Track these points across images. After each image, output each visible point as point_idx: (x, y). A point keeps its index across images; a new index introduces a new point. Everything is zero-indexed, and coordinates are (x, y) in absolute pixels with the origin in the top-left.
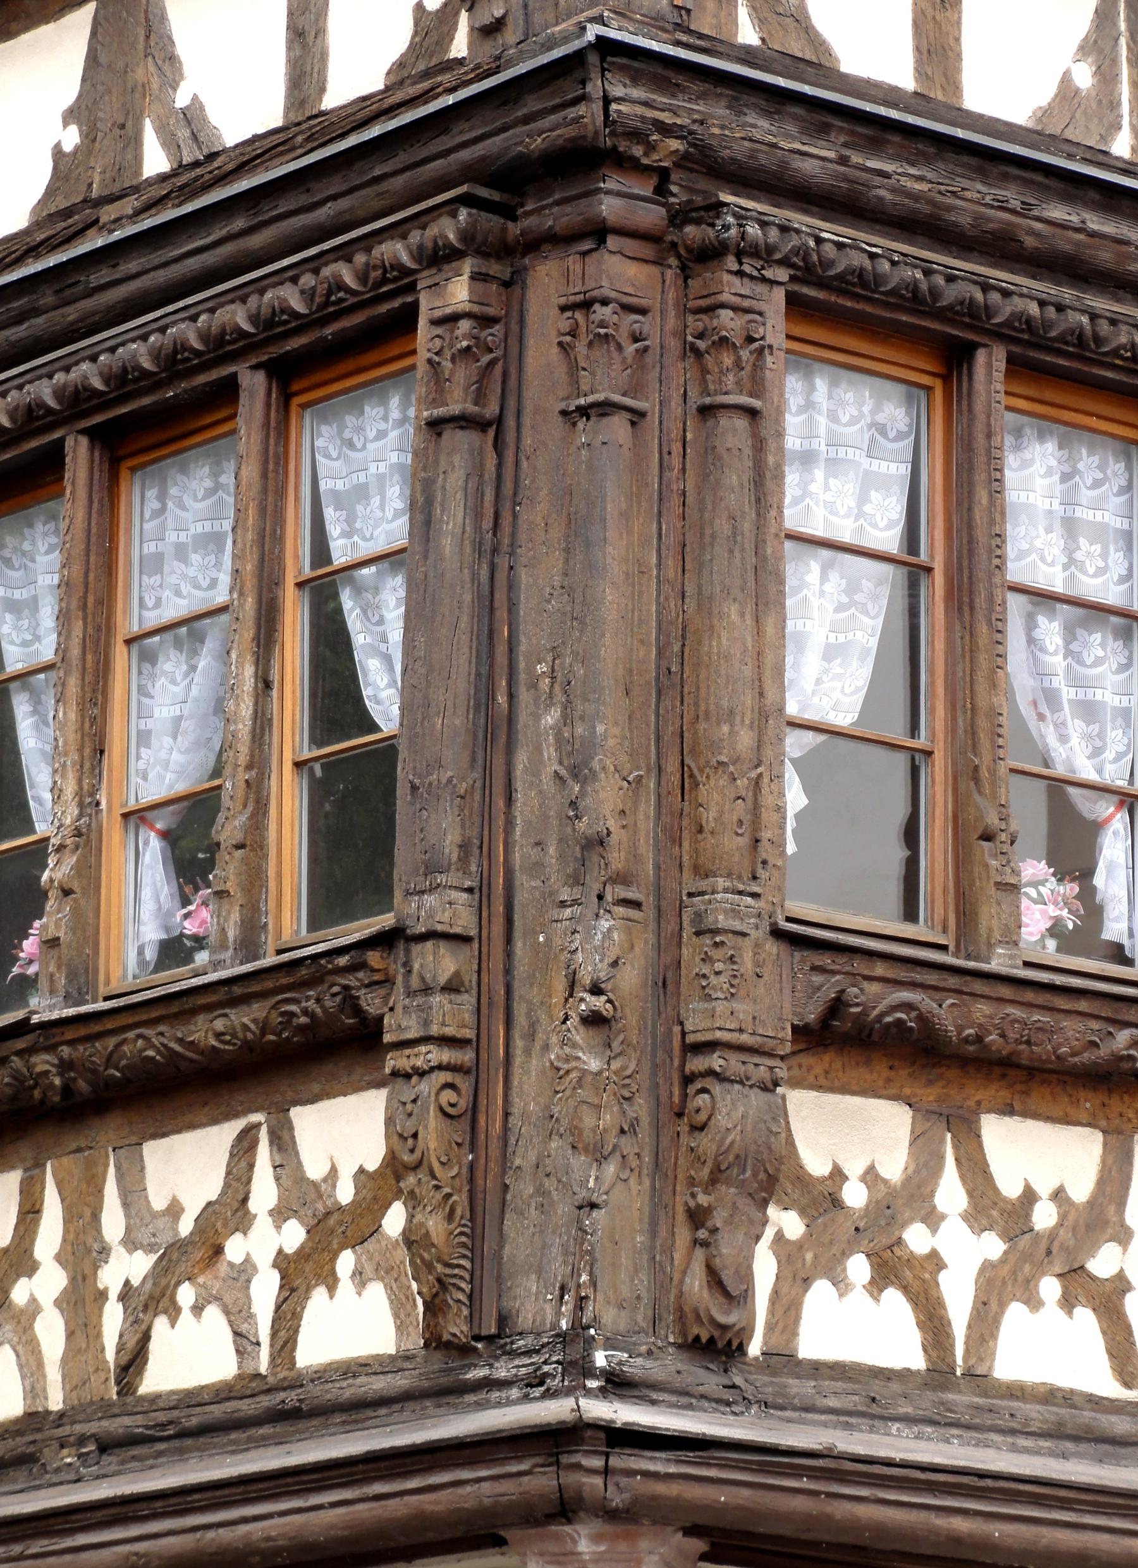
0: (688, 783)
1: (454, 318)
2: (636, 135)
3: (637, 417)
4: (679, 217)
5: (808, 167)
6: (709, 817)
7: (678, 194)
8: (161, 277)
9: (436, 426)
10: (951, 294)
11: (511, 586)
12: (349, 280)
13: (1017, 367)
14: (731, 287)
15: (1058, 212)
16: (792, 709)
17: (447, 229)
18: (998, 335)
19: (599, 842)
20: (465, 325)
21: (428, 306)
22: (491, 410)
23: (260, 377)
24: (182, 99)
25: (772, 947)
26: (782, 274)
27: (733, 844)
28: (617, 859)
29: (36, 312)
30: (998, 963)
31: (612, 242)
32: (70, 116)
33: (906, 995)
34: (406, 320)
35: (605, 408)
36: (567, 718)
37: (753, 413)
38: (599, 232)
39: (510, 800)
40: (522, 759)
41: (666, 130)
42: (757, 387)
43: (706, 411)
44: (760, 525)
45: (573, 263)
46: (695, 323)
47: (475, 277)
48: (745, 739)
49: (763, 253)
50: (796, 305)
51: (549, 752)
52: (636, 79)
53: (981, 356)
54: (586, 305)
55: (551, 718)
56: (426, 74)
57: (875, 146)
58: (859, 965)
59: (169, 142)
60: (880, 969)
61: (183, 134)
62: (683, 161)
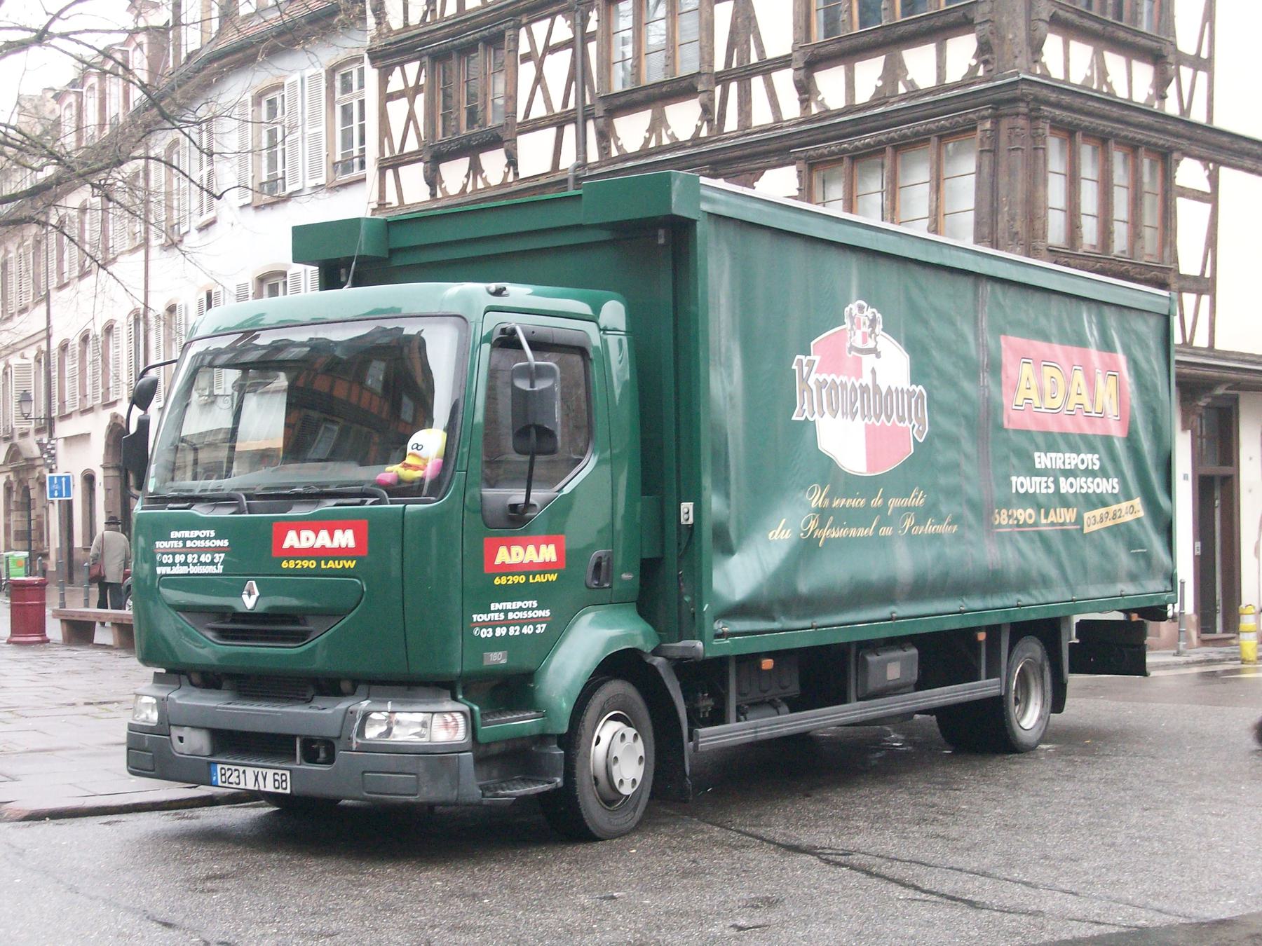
0: (1032, 221)
1: (987, 130)
2: (1026, 96)
3: (1023, 150)
4: (1031, 110)
5: (1052, 99)
6: (1036, 227)
7: (1031, 106)
8: (911, 116)
9: (982, 151)
10: (1075, 122)
11: (997, 183)
12: (961, 121)
13: (1084, 135)
14: (1042, 125)
15: (1090, 103)
16: (1050, 206)
17: (985, 113)
18: (1081, 129)
19: (1017, 233)
20: (988, 132)
21: (979, 128)
22: (993, 149)
23: (936, 139)
24: (909, 78)
25: (1047, 252)
26: (1049, 121)
27: (1041, 232)
28: (1020, 236)
29: (878, 121)
30: (1080, 252)
31: (1020, 116)
32: (879, 78)
33: (1066, 259)
34: (975, 129)
35: (1018, 149)
36: (1010, 209)
37: (1044, 149)
38: (1018, 114)
39: (997, 224)
40: (1000, 217)
41: (1031, 94)
42: (1044, 143)
43: (1035, 149)
44: (1045, 170)
45: (1011, 120)
46: (1035, 131)
47: (992, 122)
48: (1043, 213)
49: (1046, 117)
50: (1052, 127)
51: (1006, 215)
52: (1026, 84)
53: (1077, 134)
54: (1013, 128)
55: (1006, 209)
56: (972, 78)
57: (1062, 94)
58: (1059, 254)
59: (906, 86)
60: (1063, 255)
61: (909, 85)
62: (1032, 100)
